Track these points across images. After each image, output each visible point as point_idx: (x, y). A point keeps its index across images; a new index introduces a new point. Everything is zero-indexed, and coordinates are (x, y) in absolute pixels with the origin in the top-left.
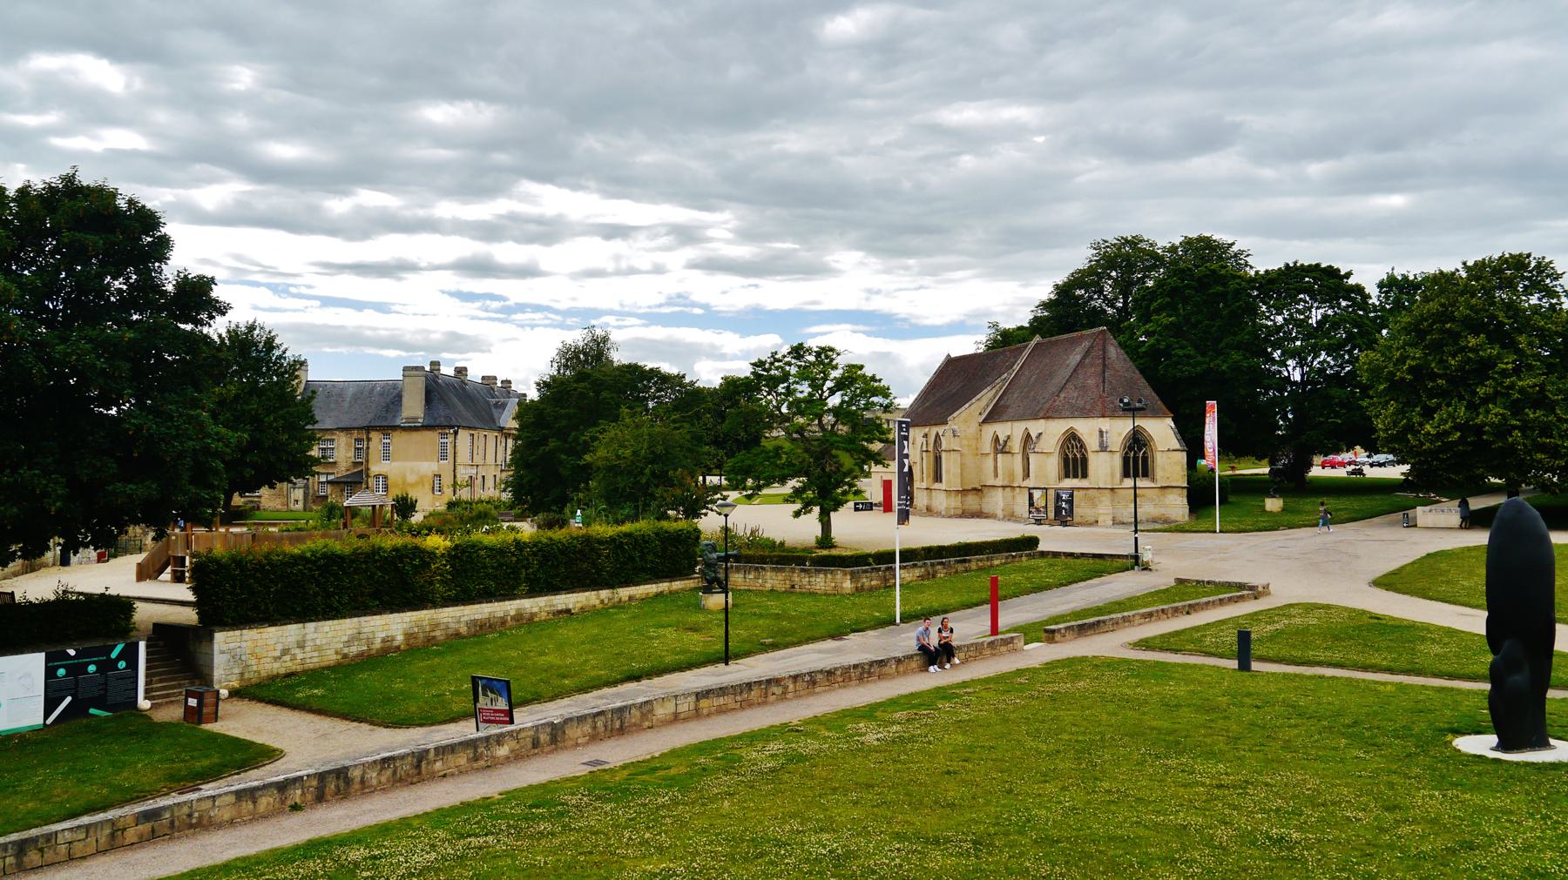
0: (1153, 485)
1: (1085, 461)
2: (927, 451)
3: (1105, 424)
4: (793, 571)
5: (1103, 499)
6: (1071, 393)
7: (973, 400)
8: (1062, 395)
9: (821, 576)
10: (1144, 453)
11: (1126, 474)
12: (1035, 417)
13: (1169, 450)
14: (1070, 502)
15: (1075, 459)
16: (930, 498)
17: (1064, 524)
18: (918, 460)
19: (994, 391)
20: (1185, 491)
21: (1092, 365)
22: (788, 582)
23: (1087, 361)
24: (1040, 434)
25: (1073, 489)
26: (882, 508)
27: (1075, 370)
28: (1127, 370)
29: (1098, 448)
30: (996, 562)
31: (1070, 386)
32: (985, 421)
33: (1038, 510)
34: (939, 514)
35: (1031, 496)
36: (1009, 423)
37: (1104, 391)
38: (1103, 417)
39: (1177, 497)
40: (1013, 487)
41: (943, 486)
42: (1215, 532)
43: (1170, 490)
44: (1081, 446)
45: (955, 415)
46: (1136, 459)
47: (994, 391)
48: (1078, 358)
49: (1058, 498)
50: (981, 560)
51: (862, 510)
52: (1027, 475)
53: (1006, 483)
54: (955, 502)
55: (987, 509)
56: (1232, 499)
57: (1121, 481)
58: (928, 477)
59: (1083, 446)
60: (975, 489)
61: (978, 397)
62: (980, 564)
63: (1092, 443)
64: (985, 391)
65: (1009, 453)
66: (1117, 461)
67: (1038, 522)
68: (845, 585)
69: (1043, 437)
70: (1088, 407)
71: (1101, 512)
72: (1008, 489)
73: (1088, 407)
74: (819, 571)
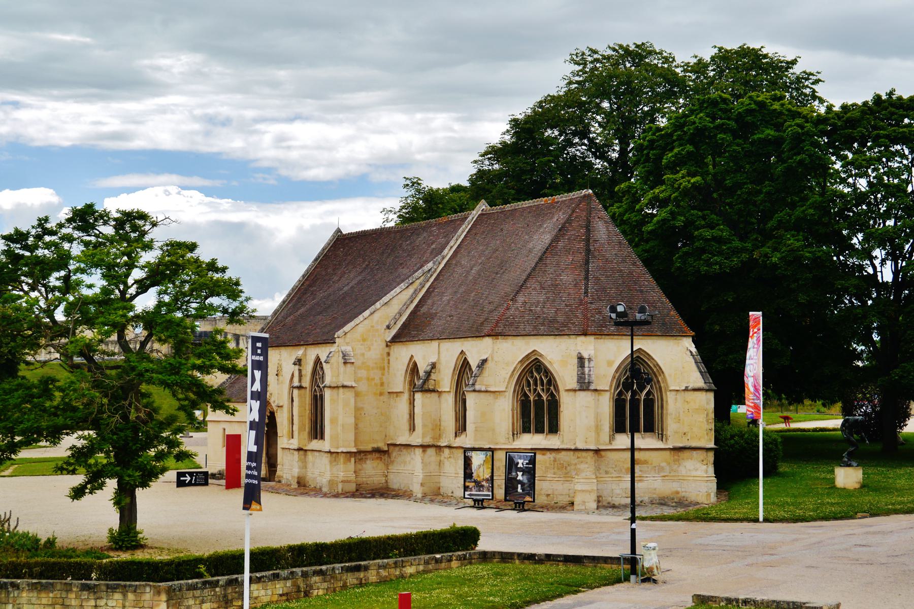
0: (660, 445)
1: (554, 405)
2: (300, 388)
3: (587, 346)
4: (68, 589)
5: (582, 466)
6: (534, 296)
7: (378, 305)
8: (521, 299)
9: (117, 596)
11: (619, 427)
12: (477, 333)
13: (686, 389)
14: (530, 471)
15: (539, 402)
16: (304, 464)
17: (520, 507)
18: (285, 402)
19: (411, 290)
20: (711, 456)
21: (568, 251)
23: (561, 244)
24: (484, 361)
25: (534, 451)
26: (223, 482)
27: (541, 259)
28: (624, 261)
30: (410, 570)
31: (532, 283)
32: (397, 339)
33: (479, 485)
34: (317, 492)
35: (467, 463)
36: (435, 344)
37: (586, 292)
38: (585, 334)
39: (699, 465)
40: (439, 448)
41: (325, 445)
42: (756, 520)
43: (687, 454)
45: (347, 328)
46: (635, 403)
47: (411, 290)
48: (547, 238)
49: (511, 465)
50: (384, 567)
51: (190, 484)
52: (461, 427)
53: (428, 440)
54: (345, 471)
55: (396, 482)
56: (784, 468)
57: (612, 438)
58: (301, 430)
59: (551, 381)
60: (377, 451)
61: (385, 299)
62: (384, 573)
63: (566, 377)
64: (398, 290)
65: (433, 391)
66: (605, 406)
67: (479, 504)
69: (488, 365)
70: (561, 318)
71: (578, 487)
72: (431, 452)
73: (561, 318)
74: (113, 589)
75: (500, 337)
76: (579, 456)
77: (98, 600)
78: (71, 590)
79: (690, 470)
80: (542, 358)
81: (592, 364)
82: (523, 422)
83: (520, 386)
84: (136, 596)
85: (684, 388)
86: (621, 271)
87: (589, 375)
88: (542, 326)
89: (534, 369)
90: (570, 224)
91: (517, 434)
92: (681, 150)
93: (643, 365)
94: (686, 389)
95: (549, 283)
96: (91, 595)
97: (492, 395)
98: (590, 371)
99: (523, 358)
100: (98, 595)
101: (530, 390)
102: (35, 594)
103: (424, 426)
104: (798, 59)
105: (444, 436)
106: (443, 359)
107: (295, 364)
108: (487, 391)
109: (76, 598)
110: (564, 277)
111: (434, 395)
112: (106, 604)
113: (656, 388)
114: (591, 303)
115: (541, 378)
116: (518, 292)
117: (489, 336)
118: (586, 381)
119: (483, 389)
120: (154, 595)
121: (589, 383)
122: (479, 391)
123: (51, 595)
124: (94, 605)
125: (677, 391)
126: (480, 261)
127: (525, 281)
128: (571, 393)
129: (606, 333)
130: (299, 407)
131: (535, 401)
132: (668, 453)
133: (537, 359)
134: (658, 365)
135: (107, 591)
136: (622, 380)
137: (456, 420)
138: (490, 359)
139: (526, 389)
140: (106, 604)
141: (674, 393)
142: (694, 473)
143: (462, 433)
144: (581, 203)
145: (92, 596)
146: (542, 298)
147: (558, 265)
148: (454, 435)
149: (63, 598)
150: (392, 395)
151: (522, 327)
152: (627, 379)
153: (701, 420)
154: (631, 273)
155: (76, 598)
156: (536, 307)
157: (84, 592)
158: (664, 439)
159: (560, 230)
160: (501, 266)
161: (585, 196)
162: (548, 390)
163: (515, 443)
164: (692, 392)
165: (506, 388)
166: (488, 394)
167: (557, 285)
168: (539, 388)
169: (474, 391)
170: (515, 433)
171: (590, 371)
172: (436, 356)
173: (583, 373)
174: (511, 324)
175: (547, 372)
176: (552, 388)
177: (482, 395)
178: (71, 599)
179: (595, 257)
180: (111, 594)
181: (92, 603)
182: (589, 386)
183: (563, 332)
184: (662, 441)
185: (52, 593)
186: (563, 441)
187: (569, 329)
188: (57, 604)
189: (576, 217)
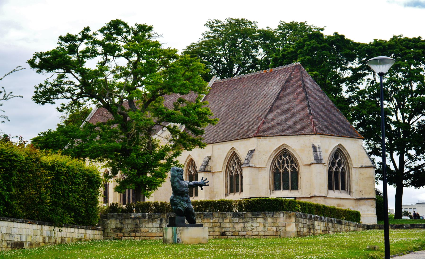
0: (348, 197)
1: (295, 175)
8: (270, 118)
9: (260, 220)
10: (343, 169)
11: (330, 187)
12: (245, 136)
13: (362, 167)
15: (286, 173)
20: (374, 203)
21: (294, 93)
22: (217, 229)
23: (288, 90)
24: (252, 152)
27: (278, 97)
28: (323, 99)
29: (312, 160)
37: (310, 113)
38: (315, 134)
39: (369, 208)
43: (362, 202)
44: (292, 162)
46: (337, 173)
48: (277, 88)
65: (210, 172)
68: (288, 229)
69: (256, 153)
70: (298, 127)
73: (298, 127)
74: (257, 216)
75: (262, 137)
76: (317, 200)
77: (246, 223)
78: (226, 217)
79: (364, 211)
81: (321, 150)
82: (275, 184)
83: (273, 164)
84: (273, 219)
85: (360, 167)
86: (323, 104)
87: (320, 156)
88: (288, 131)
89: (282, 155)
90: (291, 79)
91: (272, 191)
92: (304, 58)
93: (340, 153)
94: (362, 167)
95: (286, 109)
96: (241, 220)
97: (257, 169)
98: (320, 153)
99: (277, 148)
100: (246, 220)
101: (280, 167)
104: (325, 28)
105: (216, 197)
108: (255, 167)
109: (230, 222)
110: (294, 106)
112: (252, 225)
113: (346, 166)
114: (314, 119)
115: (287, 160)
116: (267, 114)
117: (255, 137)
118: (319, 159)
119: (253, 166)
120: (286, 218)
121: (321, 160)
122: (252, 167)
123: (211, 221)
124: (243, 226)
125: (356, 168)
126: (225, 105)
127: (271, 108)
129: (325, 134)
132: (352, 202)
133: (285, 149)
134: (348, 153)
135: (252, 217)
136: (331, 161)
137: (226, 188)
138: (256, 149)
139: (277, 166)
140: (252, 225)
141: (355, 169)
142: (367, 212)
144: (295, 69)
145: (241, 221)
146: (283, 117)
147: (289, 99)
148: (225, 195)
149: (220, 223)
151: (275, 131)
152: (333, 160)
153: (371, 183)
154: (327, 105)
155: (230, 222)
156: (281, 121)
157: (236, 218)
158: (351, 194)
159: (286, 82)
160: (245, 104)
161: (296, 66)
162: (291, 166)
164: (365, 169)
165: (266, 165)
166: (255, 169)
167: (291, 110)
168: (285, 165)
169: (249, 166)
170: (271, 190)
171: (320, 153)
172: (211, 153)
173: (317, 155)
174: (268, 131)
175: (291, 156)
176: (294, 165)
177: (253, 169)
178: (226, 223)
179: (309, 96)
180: (255, 219)
181: (242, 225)
182: (321, 161)
183: (302, 134)
184: (350, 194)
185: (212, 219)
186: (302, 193)
187: (305, 131)
188: (215, 227)
189: (294, 76)
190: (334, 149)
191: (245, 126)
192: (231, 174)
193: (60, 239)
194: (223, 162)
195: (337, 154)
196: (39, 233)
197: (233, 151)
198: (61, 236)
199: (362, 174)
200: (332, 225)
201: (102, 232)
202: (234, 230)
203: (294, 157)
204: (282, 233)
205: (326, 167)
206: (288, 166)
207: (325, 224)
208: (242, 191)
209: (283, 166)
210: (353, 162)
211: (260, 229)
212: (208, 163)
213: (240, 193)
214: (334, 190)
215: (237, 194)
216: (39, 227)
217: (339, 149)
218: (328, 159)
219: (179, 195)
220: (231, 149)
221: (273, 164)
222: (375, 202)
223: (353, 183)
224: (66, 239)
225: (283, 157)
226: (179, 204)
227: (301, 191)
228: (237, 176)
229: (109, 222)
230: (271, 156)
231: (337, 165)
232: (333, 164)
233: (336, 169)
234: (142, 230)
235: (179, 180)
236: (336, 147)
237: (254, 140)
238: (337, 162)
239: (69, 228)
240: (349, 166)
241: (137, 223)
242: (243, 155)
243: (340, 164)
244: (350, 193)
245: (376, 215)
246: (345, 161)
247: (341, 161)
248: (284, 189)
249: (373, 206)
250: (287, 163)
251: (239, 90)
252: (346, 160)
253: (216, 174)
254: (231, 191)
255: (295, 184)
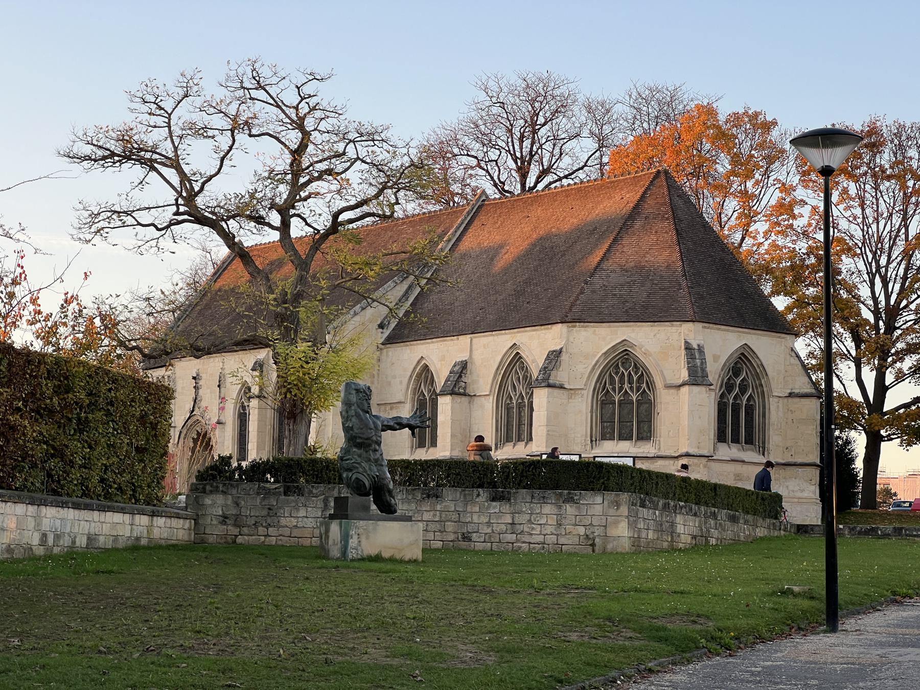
9: (548, 509)
11: (721, 437)
12: (543, 321)
13: (791, 395)
15: (625, 402)
18: (230, 416)
19: (405, 286)
20: (816, 473)
22: (450, 526)
29: (684, 375)
32: (391, 340)
36: (465, 340)
44: (641, 378)
65: (464, 394)
68: (613, 532)
69: (564, 357)
74: (544, 500)
79: (793, 491)
80: (634, 350)
82: (603, 428)
83: (601, 384)
84: (579, 508)
86: (712, 256)
91: (596, 440)
94: (791, 395)
95: (632, 264)
102: (413, 506)
103: (453, 436)
106: (478, 357)
107: (253, 369)
111: (464, 399)
112: (529, 521)
113: (758, 392)
114: (692, 288)
117: (562, 322)
120: (609, 507)
124: (510, 521)
125: (780, 397)
128: (673, 391)
130: (259, 421)
131: (620, 401)
133: (626, 350)
138: (564, 350)
141: (776, 400)
142: (799, 494)
143: (504, 444)
145: (506, 508)
150: (383, 408)
153: (810, 432)
154: (722, 260)
157: (494, 504)
158: (766, 453)
163: (593, 452)
166: (561, 391)
168: (626, 386)
172: (468, 354)
175: (638, 366)
176: (644, 385)
180: (539, 505)
184: (763, 455)
185: (440, 504)
186: (660, 448)
190: (732, 354)
191: (542, 299)
192: (508, 402)
193: (86, 537)
194: (492, 375)
195: (739, 366)
196: (31, 523)
197: (515, 352)
198: (87, 532)
199: (791, 411)
200: (716, 524)
201: (193, 521)
202: (489, 531)
203: (645, 369)
204: (597, 540)
205: (713, 394)
206: (631, 388)
207: (700, 521)
208: (531, 439)
209: (621, 389)
210: (773, 386)
211: (549, 529)
212: (460, 376)
213: (526, 444)
214: (729, 444)
215: (521, 446)
216: (32, 509)
217: (742, 354)
218: (719, 376)
219: (359, 446)
220: (511, 348)
221: (601, 384)
222: (818, 472)
223: (771, 433)
224: (102, 539)
225: (621, 369)
226: (357, 468)
227: (657, 442)
228: (520, 406)
229: (208, 501)
230: (596, 364)
231: (737, 389)
232: (729, 387)
233: (735, 398)
234: (283, 521)
235: (361, 413)
236: (737, 350)
237: (559, 329)
238: (738, 383)
239: (109, 514)
240: (763, 392)
241: (273, 505)
242: (535, 359)
243: (743, 389)
244: (763, 450)
245: (819, 501)
246: (755, 382)
247: (746, 380)
248: (622, 438)
249: (813, 482)
250: (630, 382)
251: (534, 219)
252: (759, 379)
253: (476, 399)
254: (508, 439)
255: (646, 428)
